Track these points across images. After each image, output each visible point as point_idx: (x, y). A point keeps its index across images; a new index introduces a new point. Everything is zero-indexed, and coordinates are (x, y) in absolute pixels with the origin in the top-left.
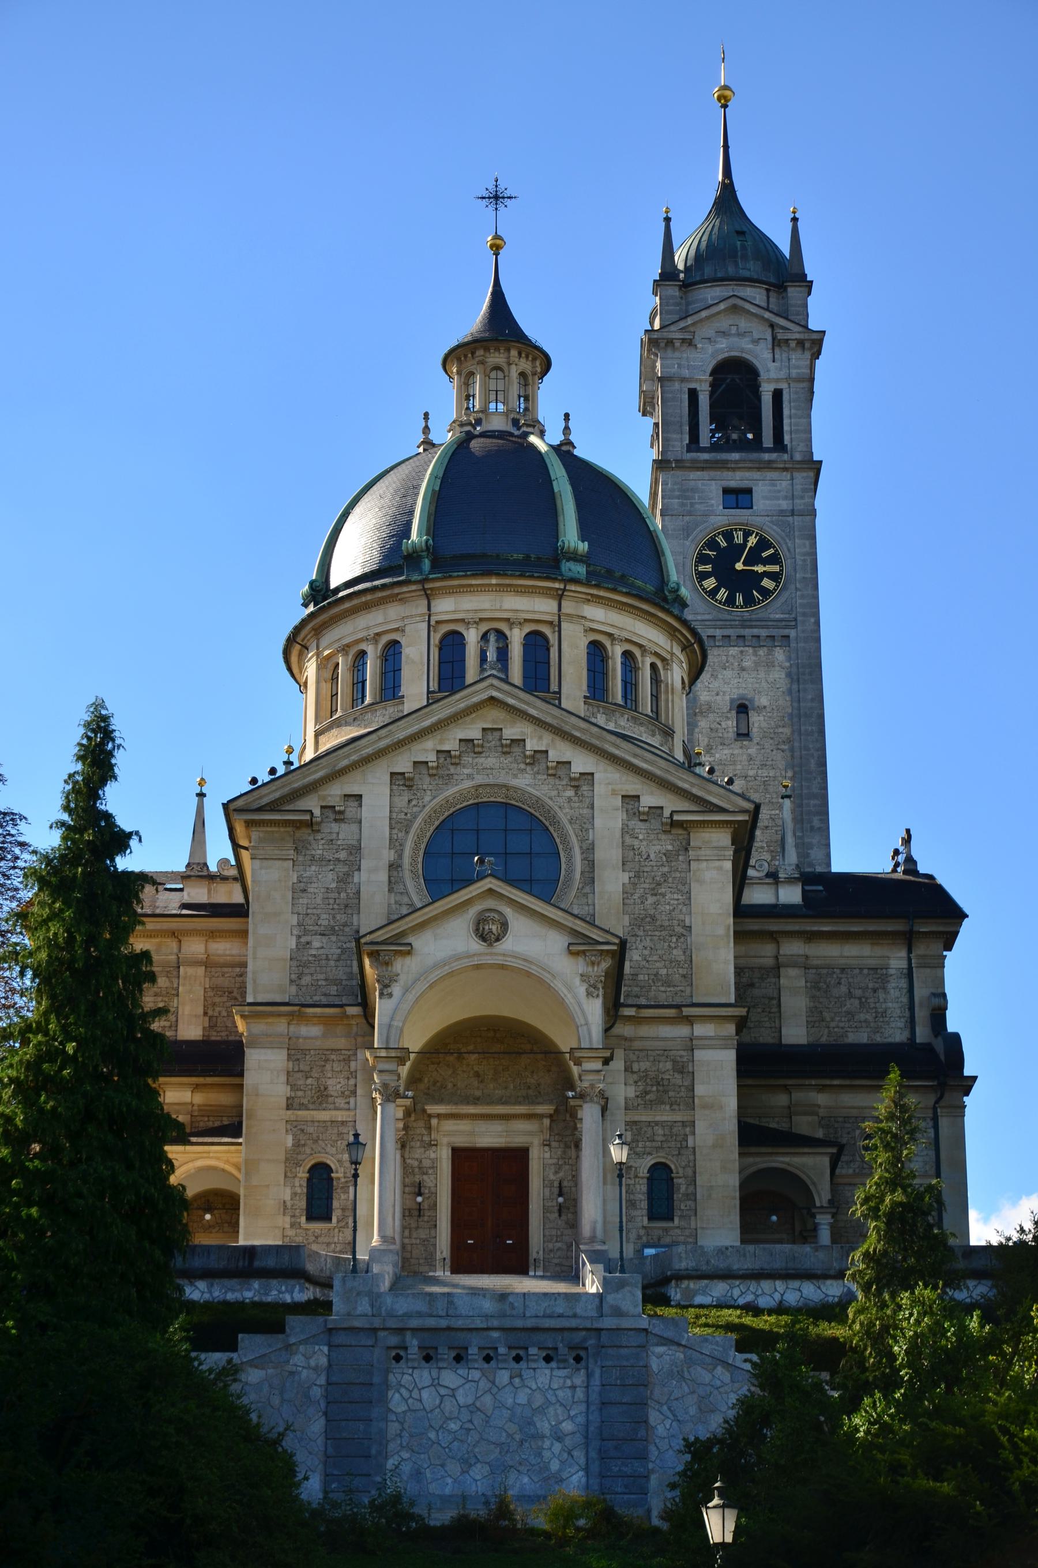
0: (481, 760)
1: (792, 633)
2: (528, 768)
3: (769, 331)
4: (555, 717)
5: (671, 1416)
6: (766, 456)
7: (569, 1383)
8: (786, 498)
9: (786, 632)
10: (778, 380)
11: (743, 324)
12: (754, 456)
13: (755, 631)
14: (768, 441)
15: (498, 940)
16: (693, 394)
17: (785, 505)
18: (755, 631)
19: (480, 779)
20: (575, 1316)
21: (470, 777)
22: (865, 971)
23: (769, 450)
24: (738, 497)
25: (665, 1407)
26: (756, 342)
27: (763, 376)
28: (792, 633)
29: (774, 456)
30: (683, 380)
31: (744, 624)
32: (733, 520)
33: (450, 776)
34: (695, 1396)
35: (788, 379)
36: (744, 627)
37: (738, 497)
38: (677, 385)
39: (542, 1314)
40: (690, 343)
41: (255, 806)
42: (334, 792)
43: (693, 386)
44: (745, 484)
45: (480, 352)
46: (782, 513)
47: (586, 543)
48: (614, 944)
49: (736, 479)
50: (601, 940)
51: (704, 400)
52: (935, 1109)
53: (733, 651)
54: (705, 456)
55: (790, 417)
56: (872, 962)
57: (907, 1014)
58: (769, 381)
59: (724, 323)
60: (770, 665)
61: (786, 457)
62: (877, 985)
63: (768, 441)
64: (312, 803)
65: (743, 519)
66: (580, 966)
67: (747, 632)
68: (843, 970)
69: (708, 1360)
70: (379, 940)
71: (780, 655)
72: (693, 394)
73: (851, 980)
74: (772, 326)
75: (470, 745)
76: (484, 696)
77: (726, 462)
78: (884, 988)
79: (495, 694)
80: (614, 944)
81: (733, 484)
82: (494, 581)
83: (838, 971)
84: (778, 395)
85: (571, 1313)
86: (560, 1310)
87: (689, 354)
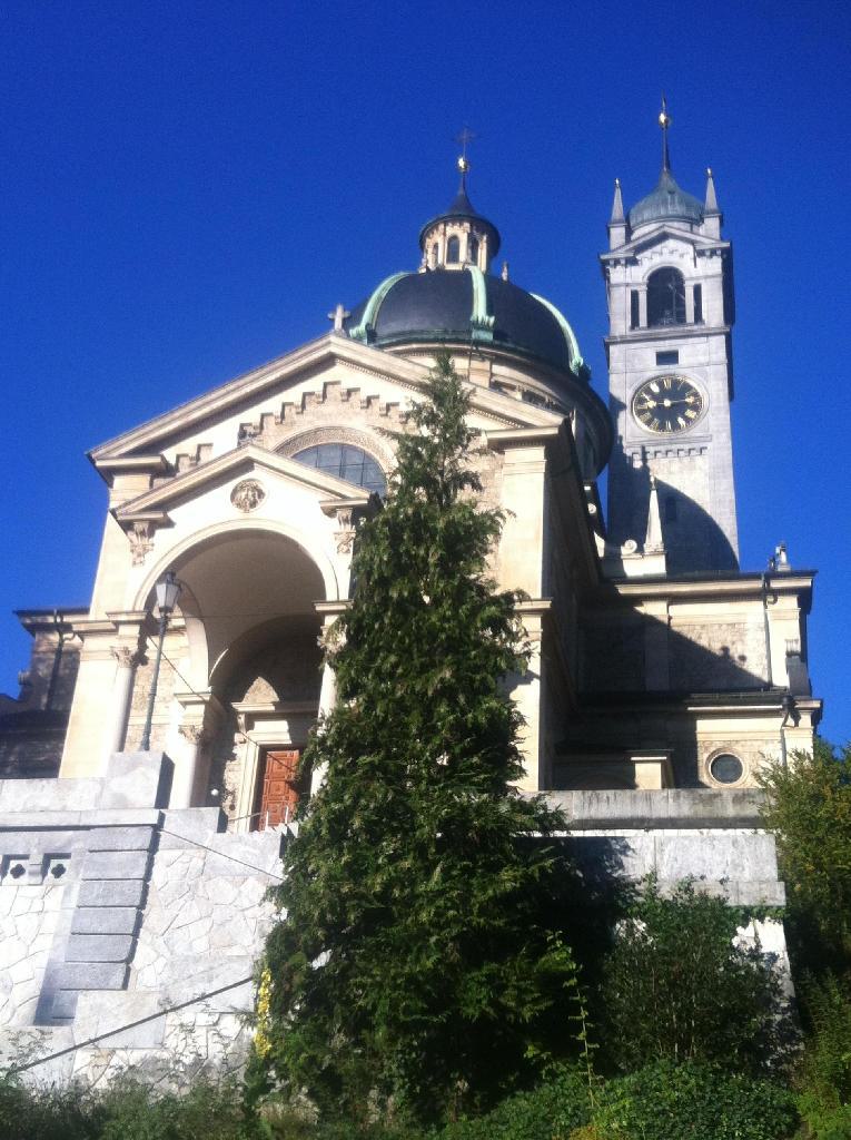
0: (322, 408)
1: (709, 445)
2: (363, 411)
3: (691, 247)
4: (385, 363)
5: (168, 955)
6: (689, 328)
7: (37, 906)
8: (705, 354)
9: (704, 445)
10: (697, 278)
11: (671, 243)
12: (680, 329)
13: (679, 446)
14: (690, 316)
15: (253, 504)
16: (635, 295)
17: (703, 359)
18: (679, 446)
19: (320, 423)
20: (64, 810)
21: (310, 422)
22: (724, 627)
23: (691, 325)
24: (667, 358)
25: (160, 941)
26: (682, 256)
27: (686, 275)
28: (709, 445)
29: (695, 327)
30: (627, 285)
31: (671, 442)
32: (662, 372)
33: (293, 423)
34: (208, 923)
35: (707, 277)
36: (671, 444)
37: (667, 358)
38: (623, 288)
39: (21, 808)
40: (632, 262)
41: (115, 454)
42: (188, 446)
43: (635, 288)
44: (673, 348)
45: (441, 227)
46: (702, 365)
47: (492, 320)
48: (364, 499)
49: (665, 346)
50: (352, 496)
51: (643, 298)
52: (782, 731)
53: (665, 461)
54: (643, 332)
55: (707, 301)
56: (730, 619)
57: (765, 662)
58: (692, 279)
59: (658, 248)
60: (692, 468)
61: (703, 327)
62: (735, 638)
63: (690, 316)
64: (170, 454)
65: (672, 372)
66: (334, 524)
67: (675, 447)
68: (703, 626)
69: (238, 868)
70: (136, 509)
71: (699, 461)
72: (635, 295)
73: (711, 635)
74: (693, 243)
75: (314, 397)
76: (323, 352)
77: (659, 334)
78: (742, 641)
79: (333, 349)
80: (364, 499)
81: (663, 349)
82: (415, 346)
83: (698, 627)
84: (697, 290)
85: (58, 807)
86: (44, 803)
87: (634, 269)
